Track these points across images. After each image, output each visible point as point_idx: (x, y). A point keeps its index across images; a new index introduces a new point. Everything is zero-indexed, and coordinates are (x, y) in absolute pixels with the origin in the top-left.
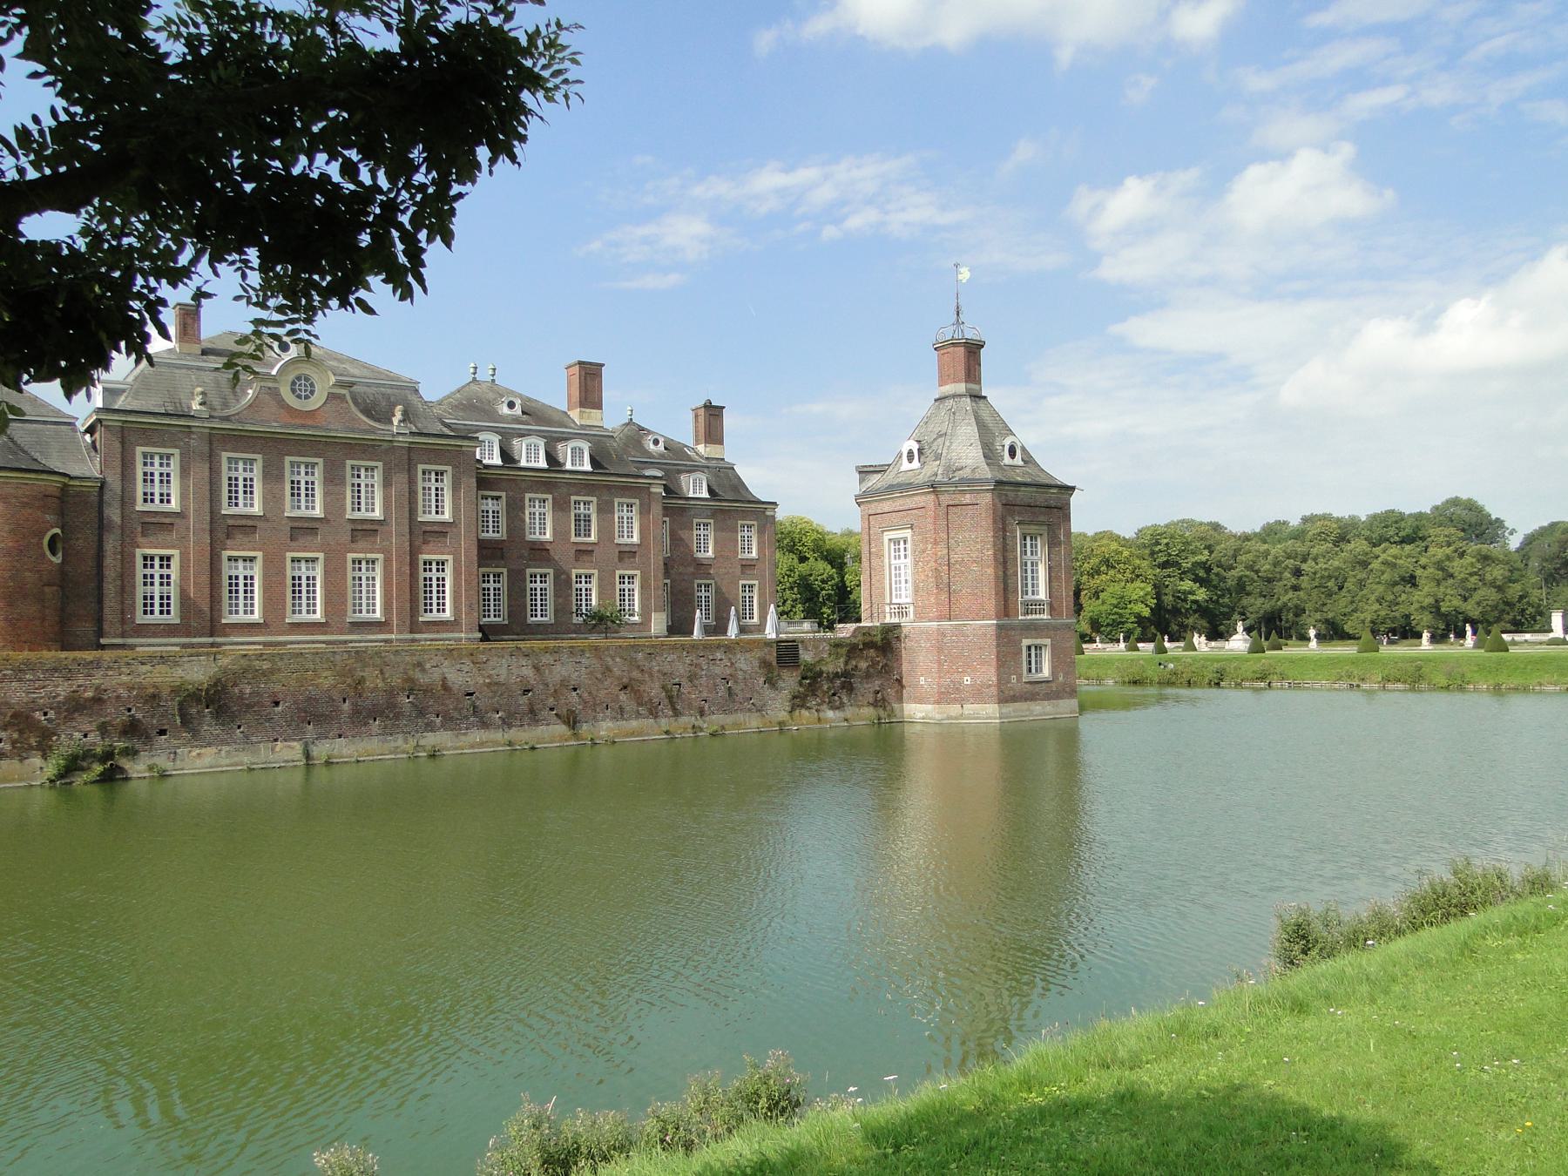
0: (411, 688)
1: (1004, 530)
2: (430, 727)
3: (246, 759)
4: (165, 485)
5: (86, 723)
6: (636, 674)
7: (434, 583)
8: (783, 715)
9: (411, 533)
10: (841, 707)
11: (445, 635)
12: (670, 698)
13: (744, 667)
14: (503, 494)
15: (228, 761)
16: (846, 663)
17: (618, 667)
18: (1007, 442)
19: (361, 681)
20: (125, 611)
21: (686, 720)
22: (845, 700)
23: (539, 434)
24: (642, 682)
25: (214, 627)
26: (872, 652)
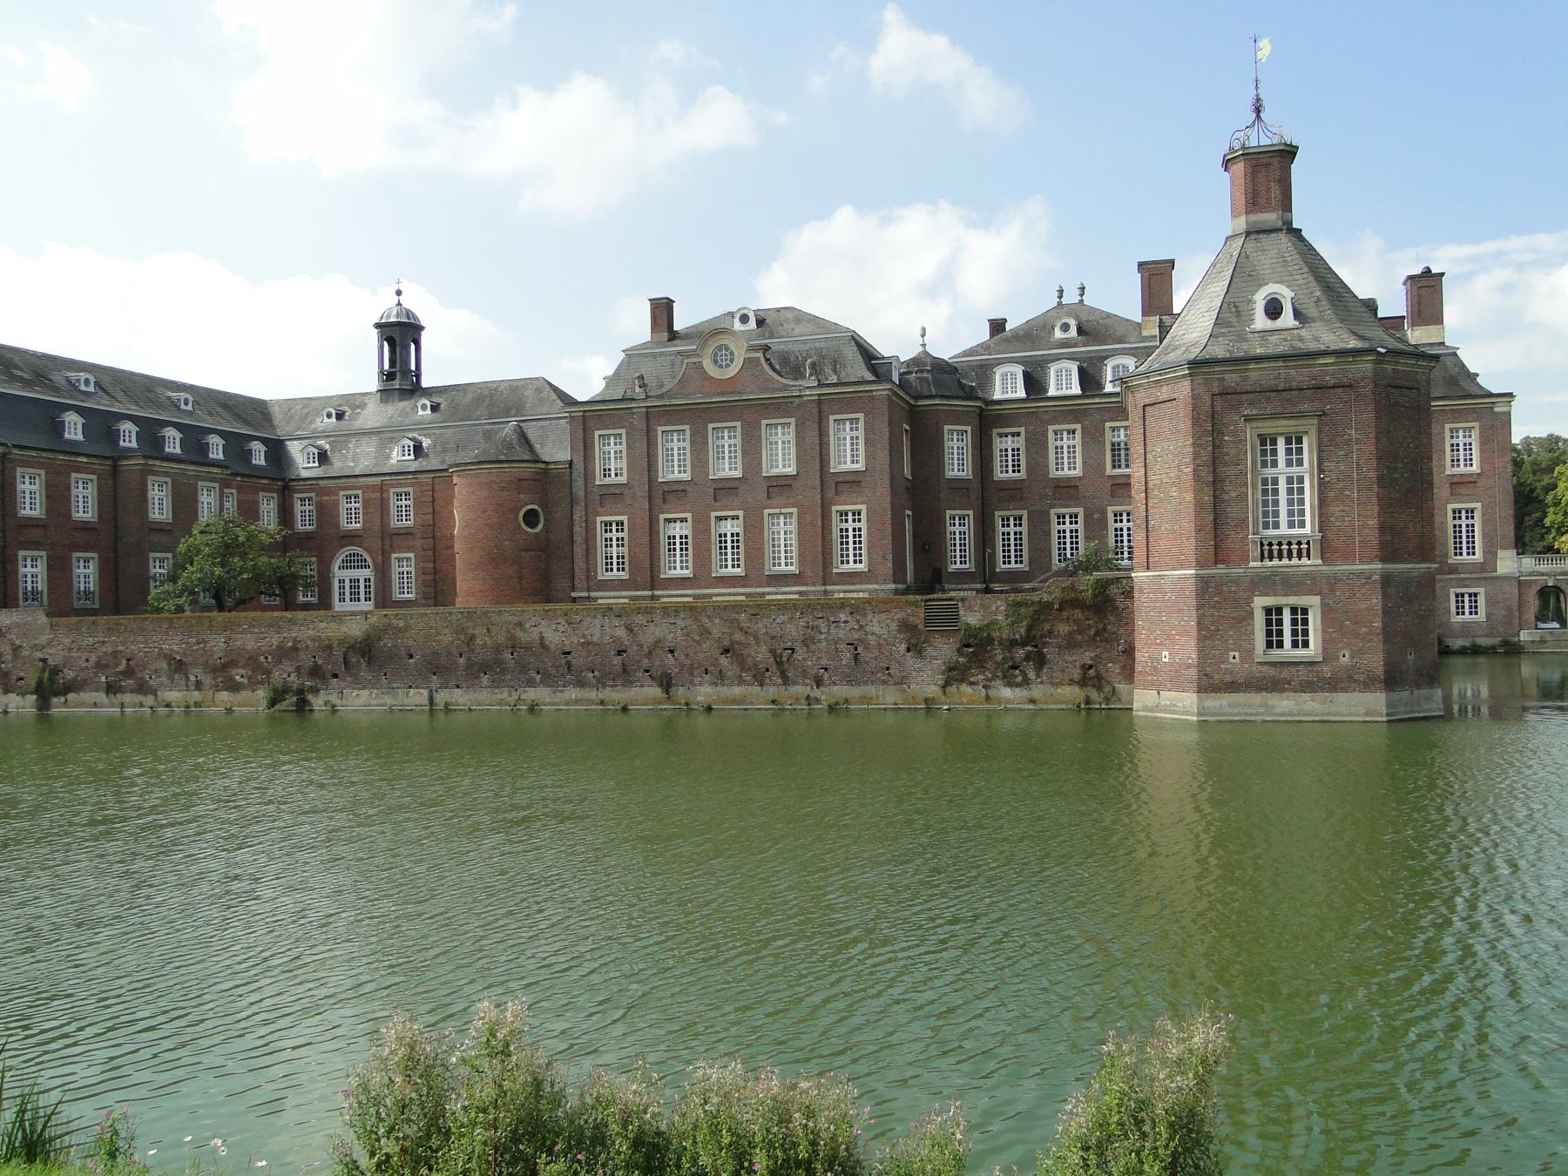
1: (1216, 432)
2: (531, 683)
3: (389, 700)
4: (613, 459)
5: (288, 666)
6: (738, 636)
7: (851, 533)
8: (933, 690)
10: (1026, 682)
12: (779, 664)
13: (877, 629)
14: (1022, 430)
15: (375, 702)
16: (1029, 628)
17: (717, 628)
18: (1260, 299)
19: (472, 638)
20: (590, 571)
21: (799, 690)
22: (1032, 675)
23: (1071, 358)
25: (654, 582)
26: (1078, 614)
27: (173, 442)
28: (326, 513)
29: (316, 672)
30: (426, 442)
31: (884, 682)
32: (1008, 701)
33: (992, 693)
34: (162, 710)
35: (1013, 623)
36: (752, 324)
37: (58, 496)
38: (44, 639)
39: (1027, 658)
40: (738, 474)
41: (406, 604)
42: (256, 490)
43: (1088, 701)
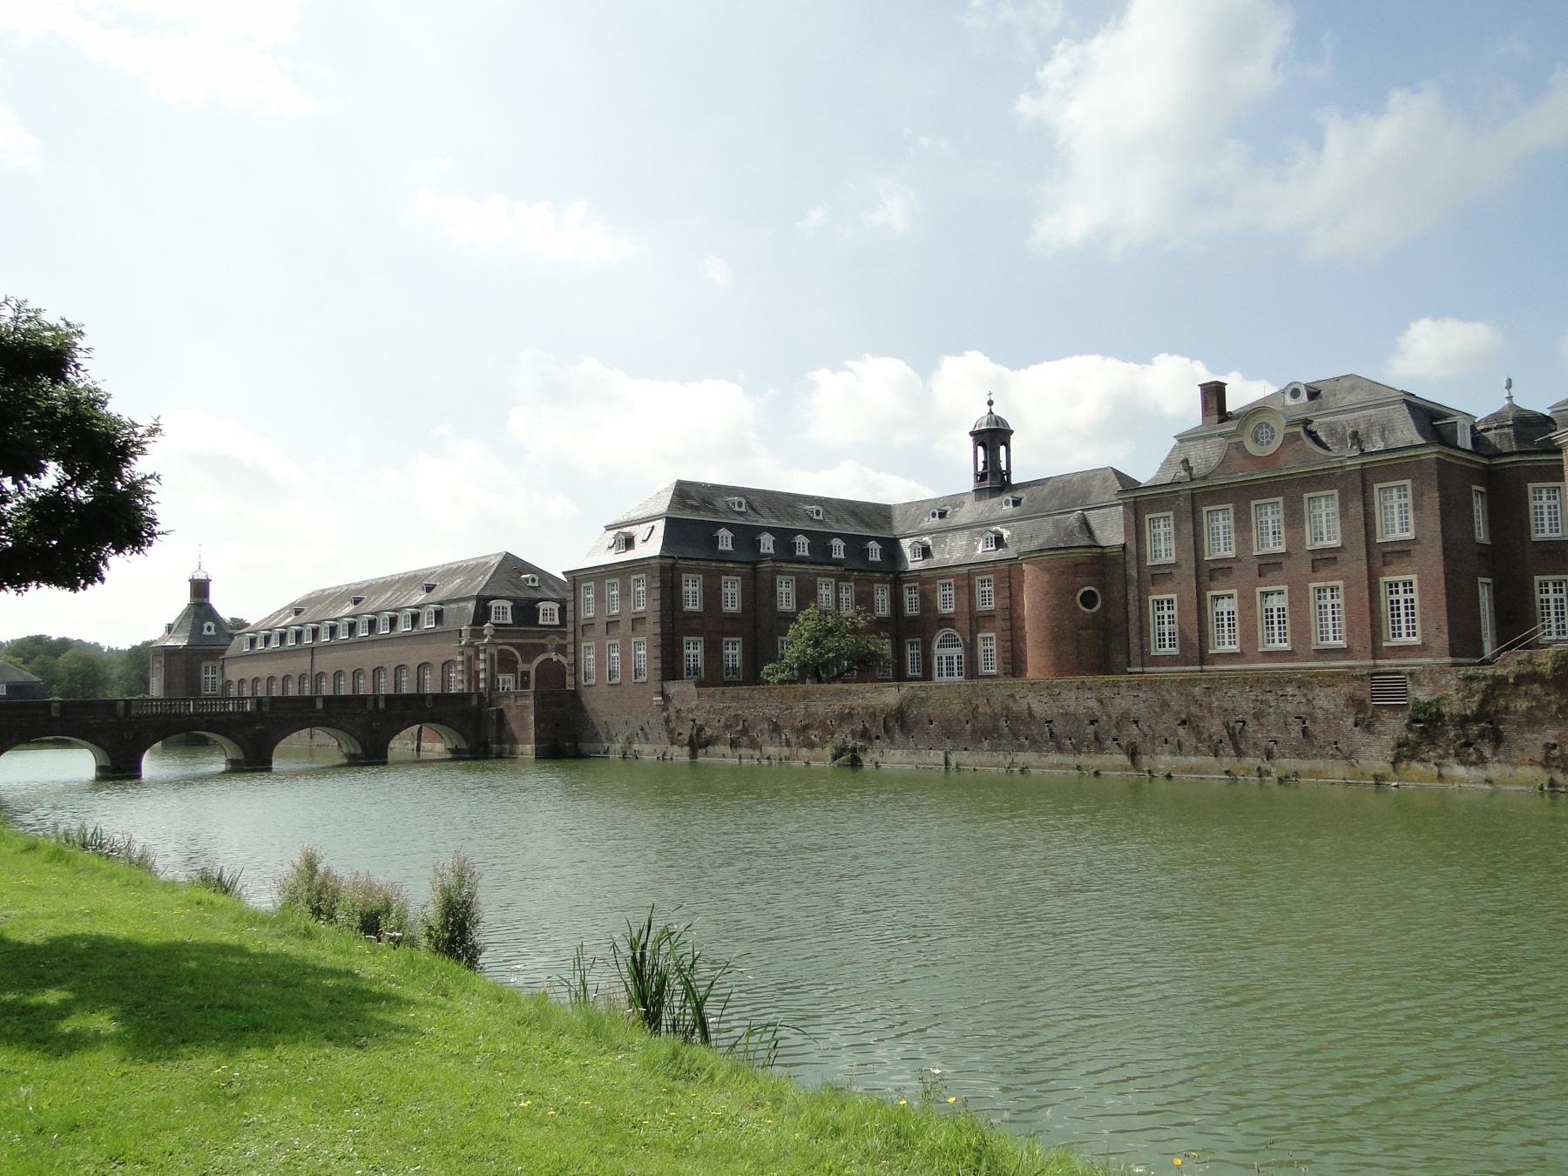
0: (1009, 716)
2: (1021, 748)
3: (915, 759)
4: (1163, 545)
5: (846, 729)
6: (1194, 709)
8: (1383, 766)
9: (1368, 553)
10: (1481, 761)
11: (1411, 661)
12: (1232, 736)
13: (1326, 705)
16: (1483, 703)
21: (1251, 762)
22: (1487, 752)
24: (1202, 718)
25: (1203, 658)
26: (1537, 689)
27: (802, 546)
28: (927, 601)
29: (865, 735)
30: (1006, 534)
31: (1333, 756)
32: (1462, 780)
33: (1445, 771)
34: (765, 762)
35: (1464, 698)
36: (1304, 397)
37: (712, 595)
38: (694, 704)
39: (1482, 736)
40: (1281, 549)
41: (991, 676)
42: (872, 583)
43: (1552, 783)
